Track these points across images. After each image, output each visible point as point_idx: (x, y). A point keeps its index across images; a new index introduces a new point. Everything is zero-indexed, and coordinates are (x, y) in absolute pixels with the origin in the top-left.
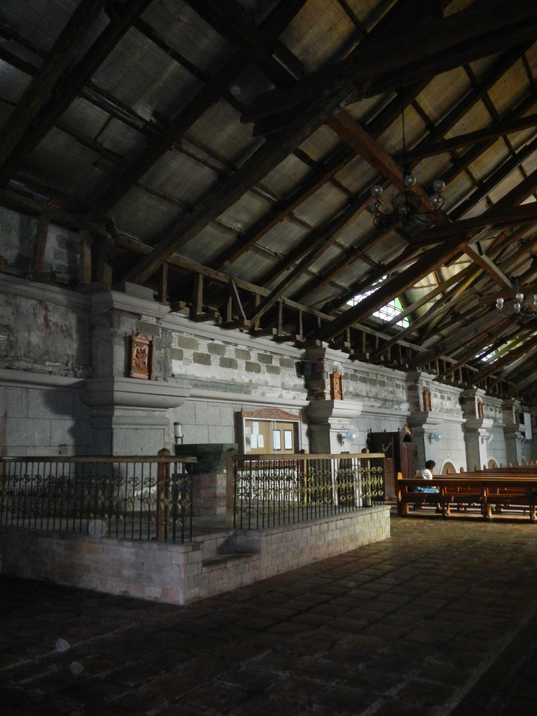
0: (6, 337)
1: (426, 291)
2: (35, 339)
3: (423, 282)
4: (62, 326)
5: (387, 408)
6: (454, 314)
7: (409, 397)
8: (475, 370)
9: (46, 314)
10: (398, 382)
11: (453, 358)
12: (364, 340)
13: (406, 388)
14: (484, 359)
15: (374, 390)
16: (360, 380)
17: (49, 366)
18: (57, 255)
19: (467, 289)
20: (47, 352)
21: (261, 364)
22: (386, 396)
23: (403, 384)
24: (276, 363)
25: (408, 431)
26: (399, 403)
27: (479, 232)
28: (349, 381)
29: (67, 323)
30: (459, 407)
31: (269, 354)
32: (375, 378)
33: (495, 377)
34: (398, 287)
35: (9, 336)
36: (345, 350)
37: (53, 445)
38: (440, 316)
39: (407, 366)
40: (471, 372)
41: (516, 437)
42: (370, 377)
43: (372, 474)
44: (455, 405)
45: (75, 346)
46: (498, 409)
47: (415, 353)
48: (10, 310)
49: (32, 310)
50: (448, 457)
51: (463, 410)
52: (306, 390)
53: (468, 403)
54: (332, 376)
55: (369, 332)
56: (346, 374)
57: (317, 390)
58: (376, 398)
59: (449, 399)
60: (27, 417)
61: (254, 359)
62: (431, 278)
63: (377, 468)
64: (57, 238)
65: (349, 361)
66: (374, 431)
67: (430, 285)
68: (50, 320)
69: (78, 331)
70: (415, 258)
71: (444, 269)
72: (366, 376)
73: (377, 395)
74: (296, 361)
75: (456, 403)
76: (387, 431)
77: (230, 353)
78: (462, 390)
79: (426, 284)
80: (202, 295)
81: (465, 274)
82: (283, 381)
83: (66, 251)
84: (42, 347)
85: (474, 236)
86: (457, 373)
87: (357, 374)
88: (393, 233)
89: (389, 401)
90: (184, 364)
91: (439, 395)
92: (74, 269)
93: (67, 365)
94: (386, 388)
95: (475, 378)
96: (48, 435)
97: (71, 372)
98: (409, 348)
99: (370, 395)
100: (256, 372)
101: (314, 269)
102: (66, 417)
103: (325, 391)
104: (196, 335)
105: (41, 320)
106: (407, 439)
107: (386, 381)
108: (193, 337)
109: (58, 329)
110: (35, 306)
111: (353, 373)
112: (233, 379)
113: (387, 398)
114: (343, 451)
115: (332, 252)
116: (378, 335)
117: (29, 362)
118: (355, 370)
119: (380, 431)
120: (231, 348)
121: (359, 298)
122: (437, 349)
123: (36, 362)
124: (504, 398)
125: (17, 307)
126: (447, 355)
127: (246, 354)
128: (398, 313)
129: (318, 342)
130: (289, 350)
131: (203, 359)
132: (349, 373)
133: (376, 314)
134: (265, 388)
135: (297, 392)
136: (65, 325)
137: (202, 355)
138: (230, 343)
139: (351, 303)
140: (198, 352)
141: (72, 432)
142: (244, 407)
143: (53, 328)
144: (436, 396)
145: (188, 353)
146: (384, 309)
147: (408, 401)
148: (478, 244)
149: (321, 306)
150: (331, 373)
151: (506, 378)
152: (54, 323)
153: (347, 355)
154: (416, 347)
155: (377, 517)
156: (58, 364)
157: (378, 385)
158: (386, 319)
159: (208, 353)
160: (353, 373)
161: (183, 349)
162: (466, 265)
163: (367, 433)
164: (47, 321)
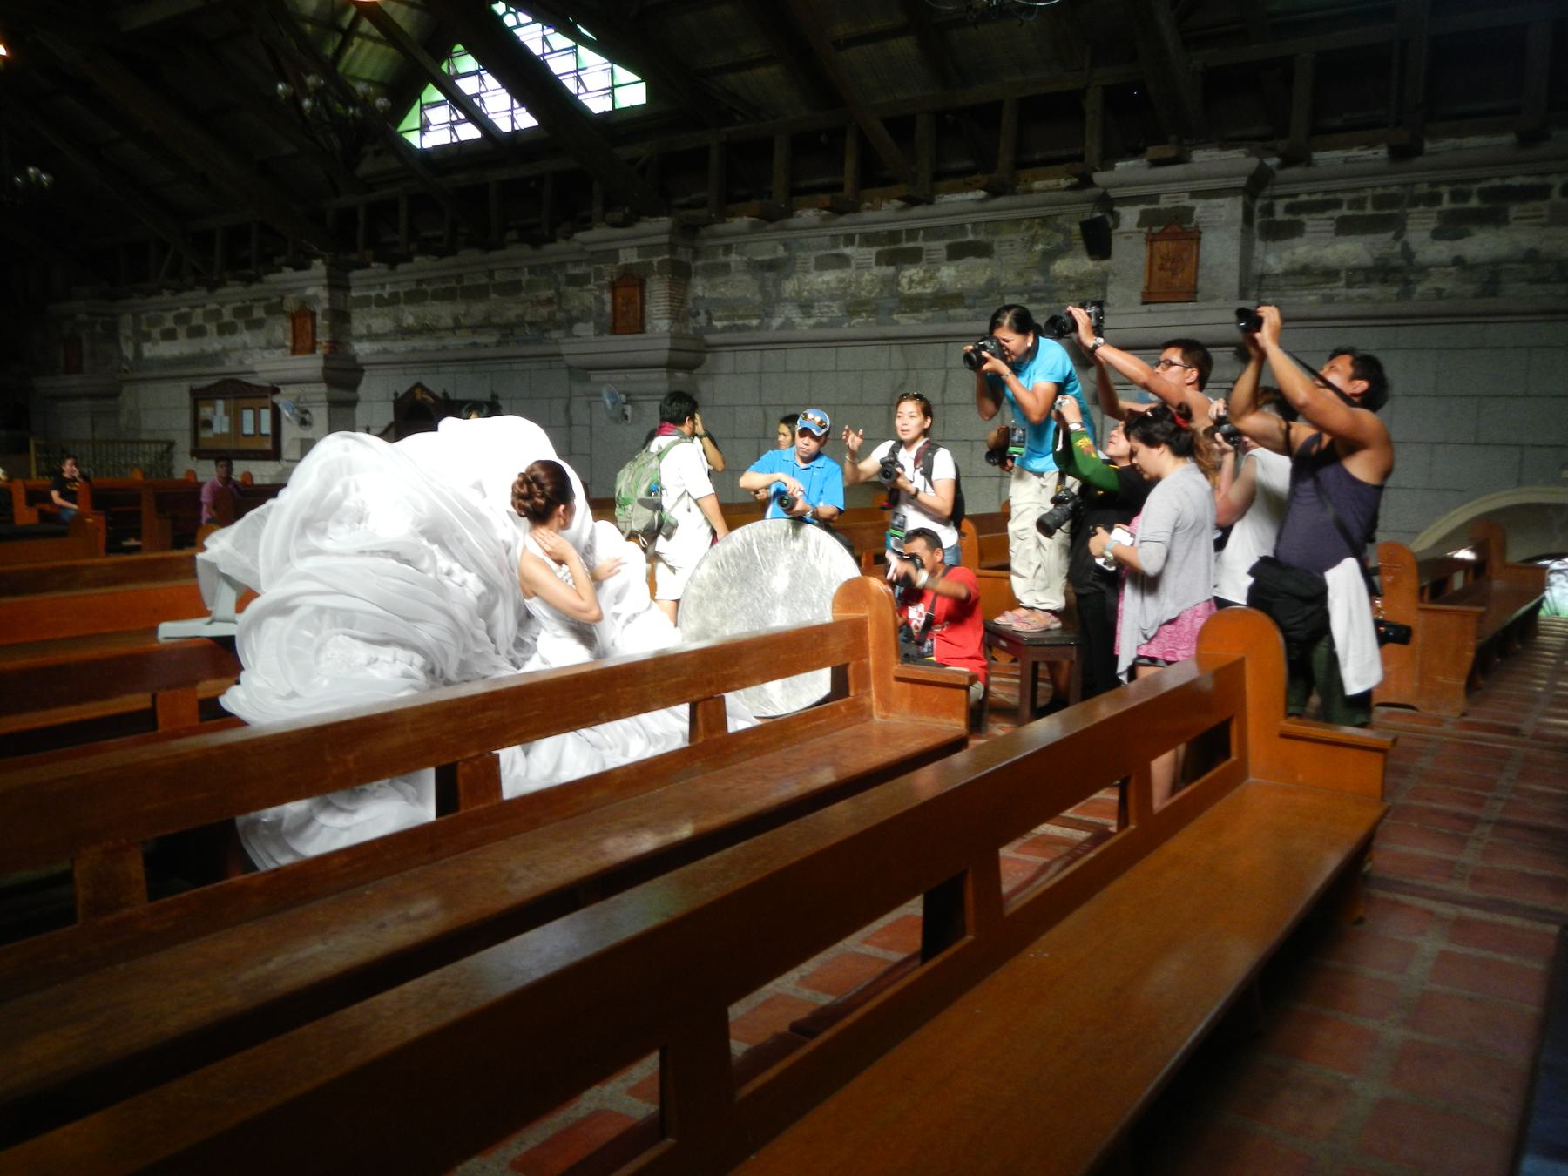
5: (526, 342)
10: (578, 271)
15: (479, 309)
24: (259, 313)
28: (402, 306)
32: (484, 281)
58: (485, 325)
61: (227, 315)
72: (453, 284)
77: (197, 319)
107: (525, 277)
111: (413, 286)
118: (420, 282)
120: (199, 311)
127: (216, 315)
131: (169, 335)
145: (156, 332)
157: (493, 296)
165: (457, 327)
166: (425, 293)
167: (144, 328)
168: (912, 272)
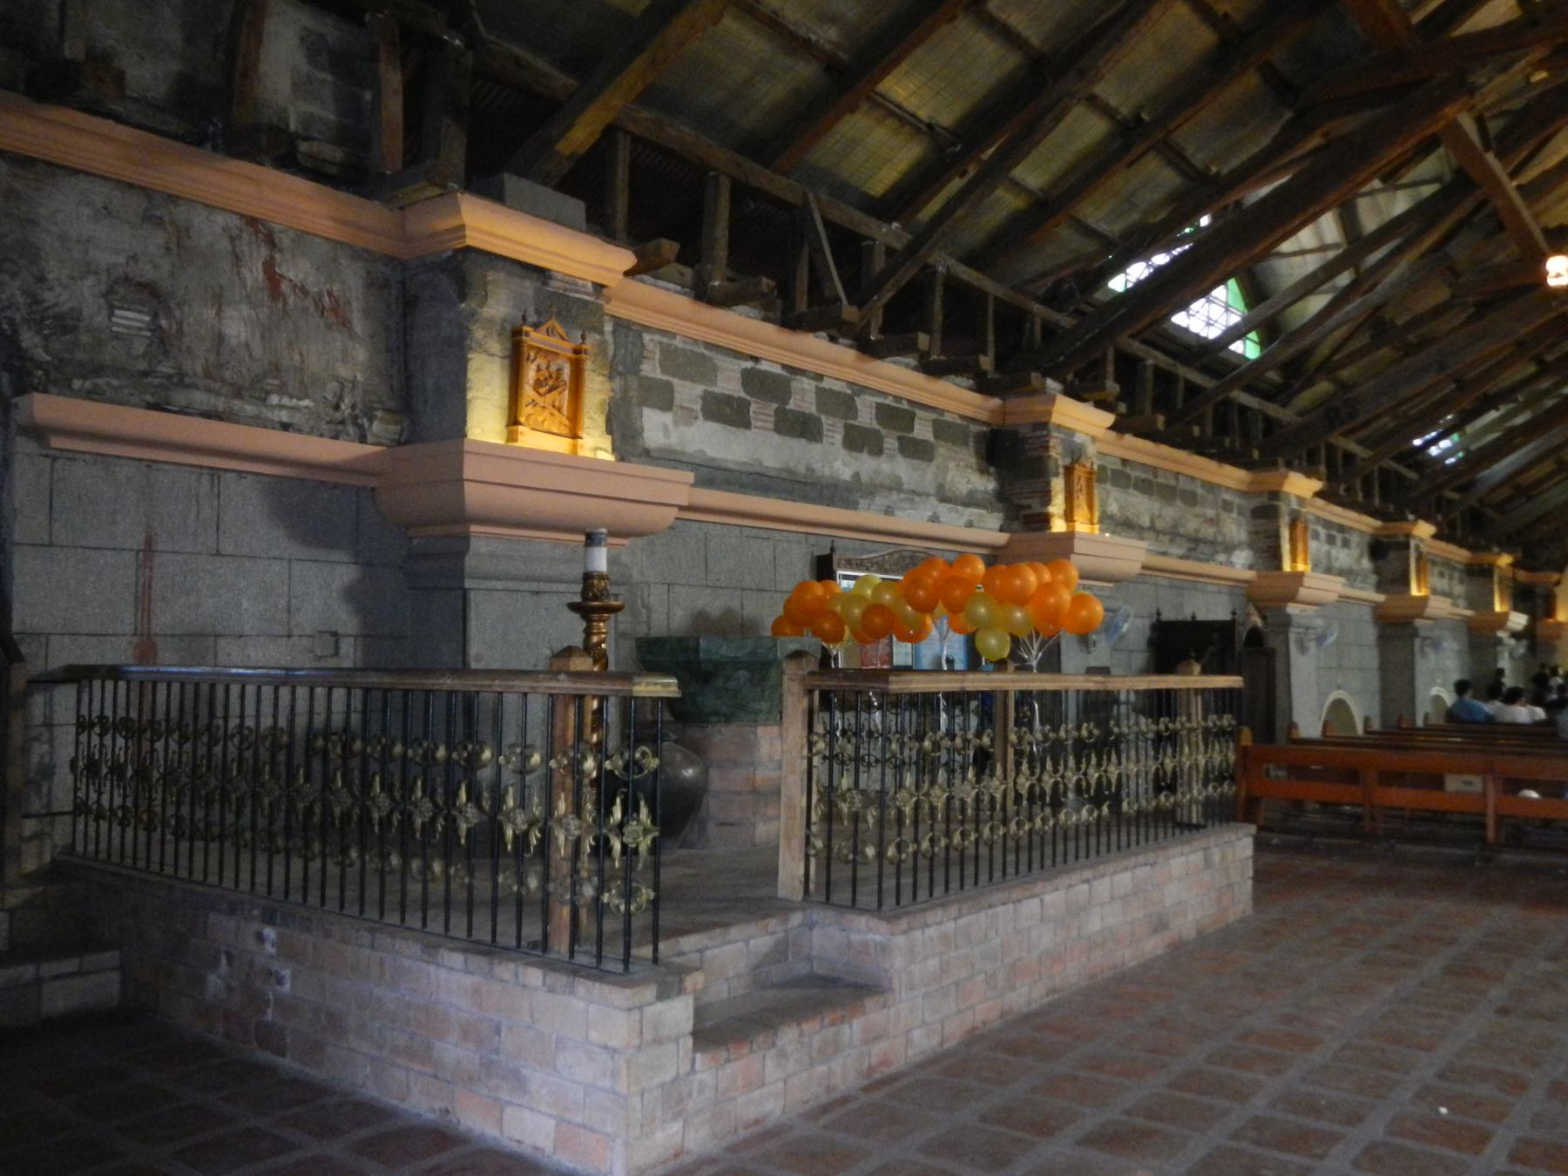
0: (147, 318)
1: (1311, 263)
2: (237, 326)
3: (1305, 237)
4: (320, 295)
5: (1200, 560)
6: (1377, 325)
7: (1254, 533)
8: (1412, 475)
9: (272, 258)
10: (1227, 496)
11: (1361, 443)
12: (1149, 385)
13: (1248, 514)
14: (1434, 451)
15: (1171, 513)
16: (1136, 487)
17: (280, 406)
18: (302, 87)
19: (1422, 256)
20: (275, 369)
21: (884, 432)
22: (1197, 530)
23: (1237, 500)
24: (922, 430)
25: (1257, 620)
26: (1229, 548)
27: (1504, 69)
28: (1108, 486)
29: (336, 288)
30: (1366, 564)
31: (905, 406)
32: (1172, 482)
33: (1455, 496)
34: (1236, 251)
35: (155, 316)
36: (1102, 405)
37: (296, 632)
38: (1345, 328)
39: (1256, 454)
40: (1399, 476)
41: (1499, 642)
42: (1161, 480)
43: (1206, 731)
44: (1358, 560)
45: (361, 354)
46: (1456, 575)
47: (1270, 424)
48: (158, 238)
49: (225, 244)
50: (1339, 687)
51: (1377, 571)
52: (1001, 505)
53: (1392, 555)
54: (1069, 471)
55: (1162, 365)
56: (1102, 468)
57: (1029, 507)
58: (1174, 534)
59: (1346, 544)
60: (218, 554)
61: (866, 417)
62: (1328, 227)
63: (1220, 718)
64: (302, 39)
65: (1112, 435)
66: (1169, 615)
67: (1323, 248)
68: (282, 276)
69: (367, 312)
70: (1303, 157)
71: (1363, 205)
72: (1151, 477)
73: (1175, 526)
74: (974, 428)
75: (1361, 556)
76: (1201, 617)
78: (1378, 523)
79: (1311, 243)
80: (726, 232)
81: (1424, 215)
82: (940, 480)
83: (330, 78)
84: (257, 350)
85: (1490, 79)
86: (1367, 481)
87: (1128, 470)
88: (1251, 80)
89: (1205, 541)
90: (676, 423)
91: (1322, 532)
92: (355, 132)
93: (337, 407)
94: (1197, 510)
95: (1414, 494)
96: (283, 602)
97: (351, 429)
98: (1261, 411)
99: (1159, 524)
100: (871, 453)
101: (1033, 174)
102: (335, 556)
103: (1052, 509)
104: (708, 345)
105: (254, 274)
106: (1255, 637)
107: (1200, 491)
108: (701, 350)
109: (309, 303)
110: (235, 232)
111: (1119, 466)
112: (810, 470)
113: (1201, 535)
114: (1093, 664)
115: (1082, 130)
116: (1185, 373)
117: (218, 394)
118: (1125, 462)
119: (1180, 618)
121: (1138, 271)
122: (1332, 415)
123: (238, 394)
124: (1472, 548)
125: (181, 234)
126: (1346, 434)
128: (1235, 319)
129: (1035, 376)
130: (956, 397)
132: (1109, 466)
133: (1179, 319)
134: (895, 496)
135: (976, 511)
136: (330, 294)
137: (728, 400)
138: (802, 372)
139: (1118, 284)
140: (716, 390)
141: (351, 595)
142: (838, 543)
143: (291, 300)
144: (1316, 536)
145: (688, 392)
146: (1198, 306)
147: (1251, 546)
148: (1480, 121)
149: (1043, 287)
150: (1068, 461)
151: (1481, 501)
152: (295, 286)
153: (1109, 419)
154: (1273, 410)
155: (1223, 858)
156: (306, 402)
157: (1178, 502)
158: (1203, 334)
159: (742, 394)
160: (1119, 466)
161: (675, 381)
162: (1427, 191)
163: (1147, 622)
164: (273, 277)
165: (1152, 528)
166: (1128, 477)
167: (651, 369)
168: (1334, 552)
